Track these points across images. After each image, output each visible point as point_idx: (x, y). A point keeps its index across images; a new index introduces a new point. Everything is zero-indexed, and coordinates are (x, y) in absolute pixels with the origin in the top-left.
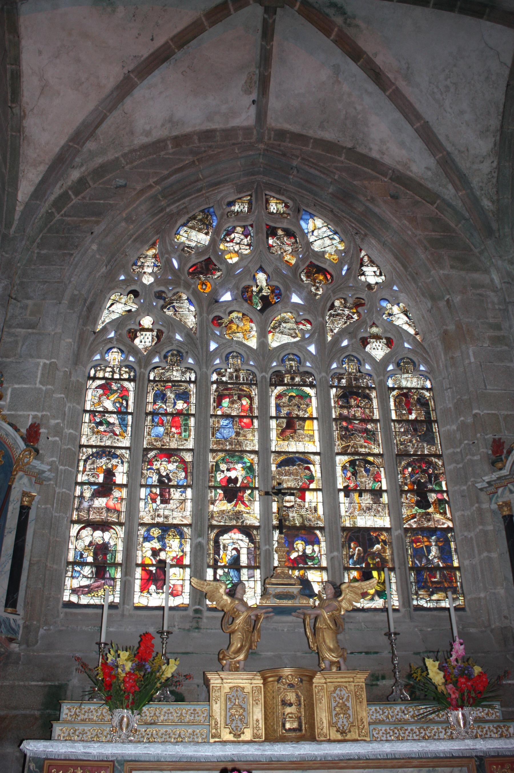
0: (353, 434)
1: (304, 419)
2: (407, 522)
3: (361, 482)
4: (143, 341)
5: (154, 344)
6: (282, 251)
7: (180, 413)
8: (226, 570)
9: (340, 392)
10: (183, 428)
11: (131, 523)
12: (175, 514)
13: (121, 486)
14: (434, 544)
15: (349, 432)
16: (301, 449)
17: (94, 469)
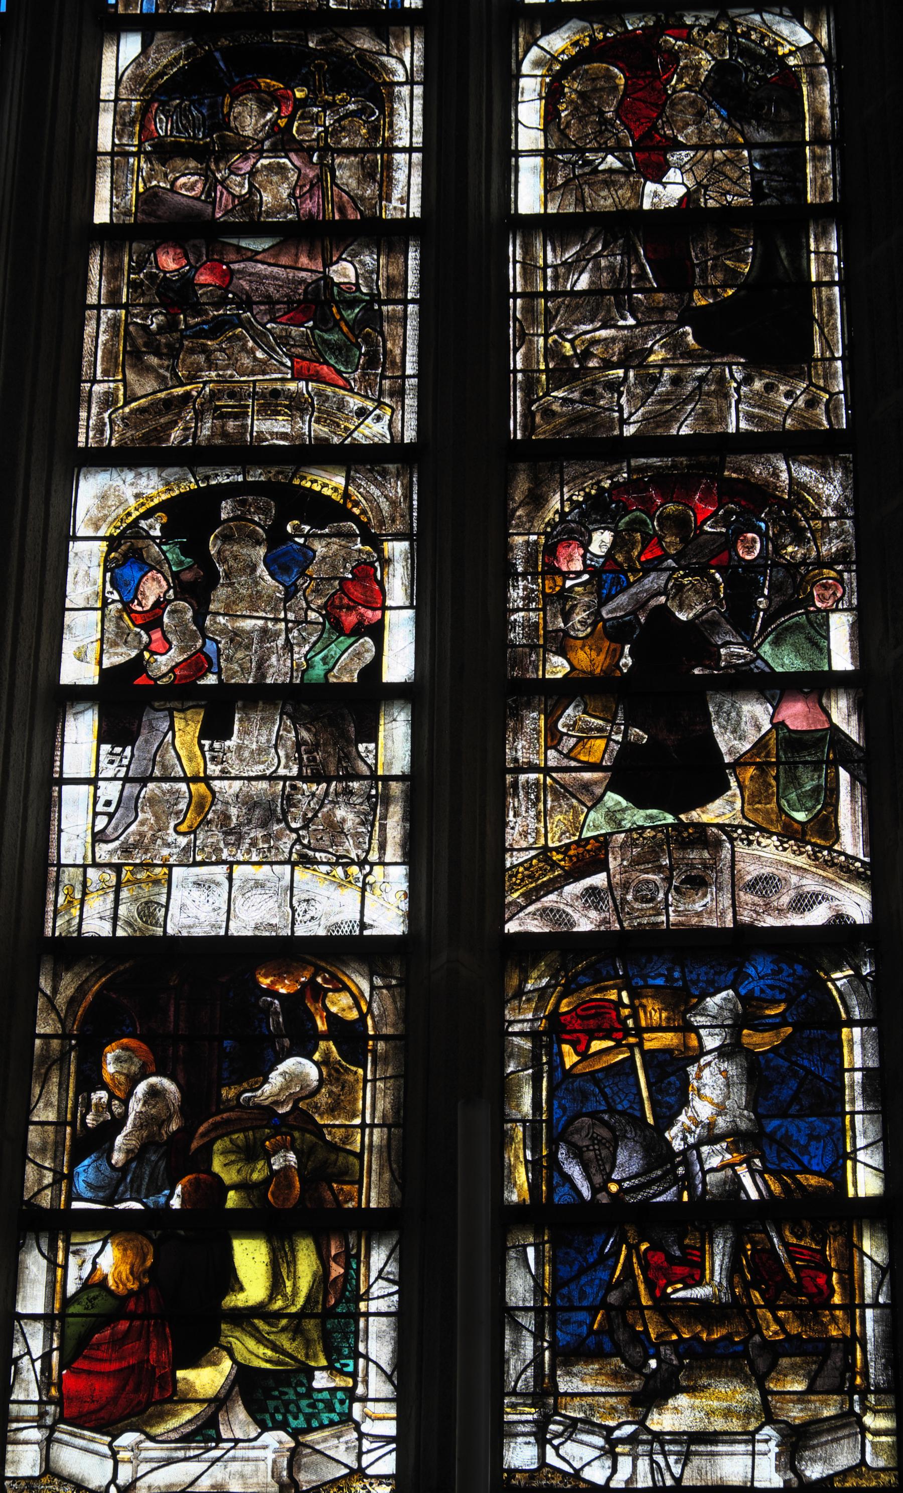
0: (218, 327)
2: (531, 897)
3: (235, 636)
9: (170, 53)
14: (711, 1042)
15: (197, 309)
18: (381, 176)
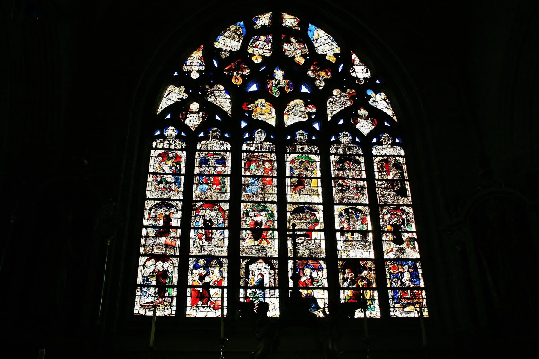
0: (347, 189)
1: (311, 178)
4: (192, 121)
5: (199, 123)
6: (295, 54)
7: (219, 174)
8: (254, 290)
9: (337, 157)
10: (221, 186)
11: (184, 255)
12: (216, 249)
13: (177, 228)
16: (309, 200)
17: (156, 216)
18: (361, 173)
